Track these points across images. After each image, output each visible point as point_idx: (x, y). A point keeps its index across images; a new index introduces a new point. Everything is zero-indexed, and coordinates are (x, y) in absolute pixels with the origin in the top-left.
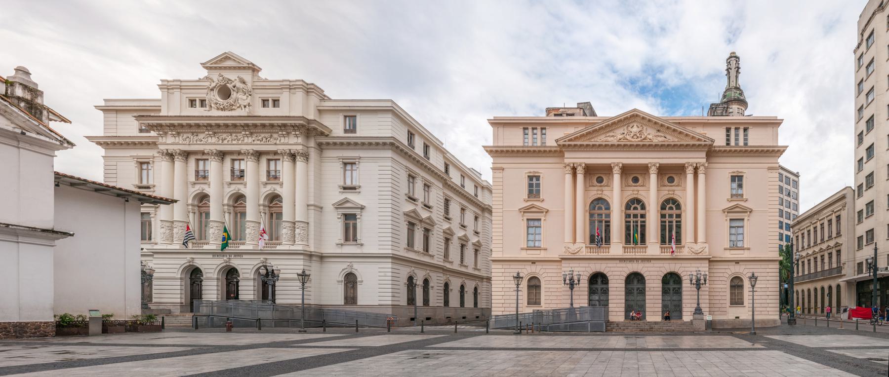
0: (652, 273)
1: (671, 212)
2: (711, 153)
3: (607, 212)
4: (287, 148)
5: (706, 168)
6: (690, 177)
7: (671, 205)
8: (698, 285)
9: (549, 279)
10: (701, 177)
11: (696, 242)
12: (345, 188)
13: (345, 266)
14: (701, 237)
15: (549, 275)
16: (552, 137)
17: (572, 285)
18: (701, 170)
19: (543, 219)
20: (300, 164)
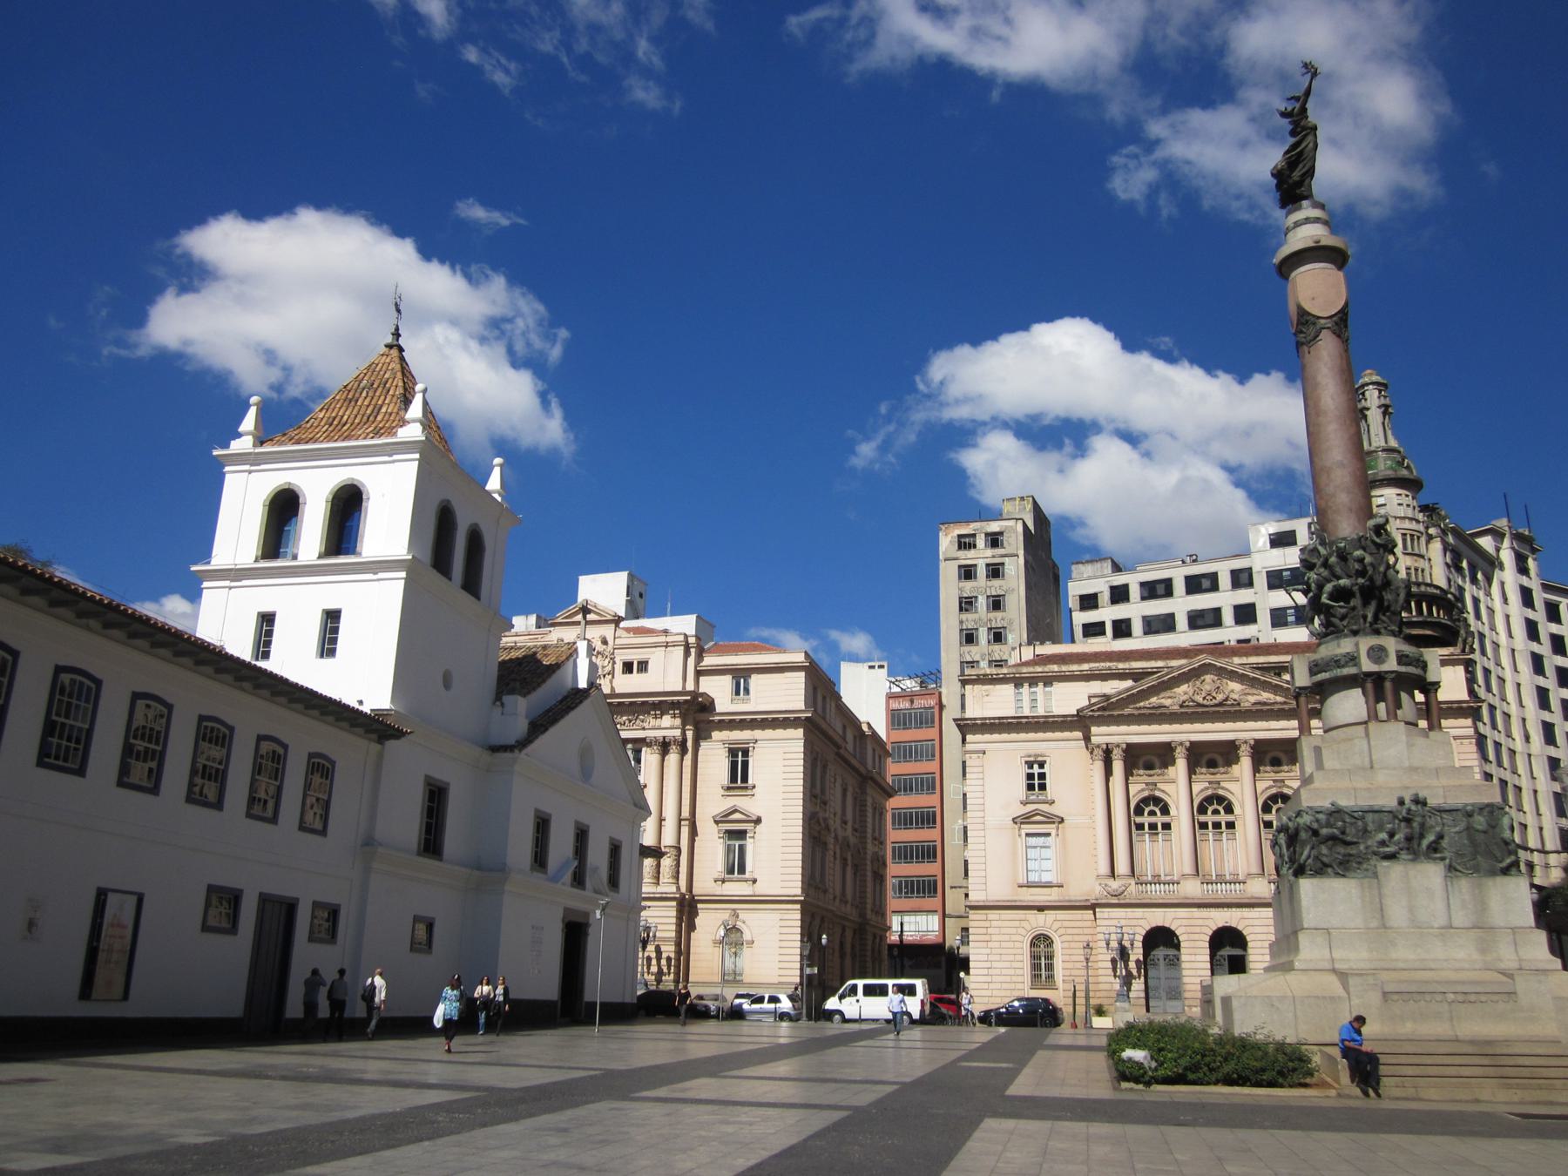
0: (1258, 929)
4: (659, 734)
12: (729, 788)
13: (726, 915)
16: (1069, 698)
19: (1053, 832)
20: (673, 757)
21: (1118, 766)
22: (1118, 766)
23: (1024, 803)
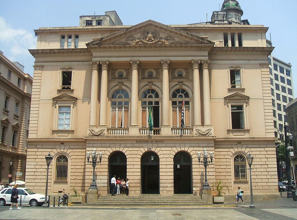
1: (181, 99)
2: (213, 51)
3: (126, 100)
5: (209, 64)
6: (196, 72)
7: (181, 94)
8: (206, 164)
9: (75, 157)
10: (206, 72)
11: (203, 124)
14: (207, 121)
15: (75, 154)
17: (94, 163)
18: (205, 66)
21: (104, 73)
22: (104, 73)
23: (59, 91)
